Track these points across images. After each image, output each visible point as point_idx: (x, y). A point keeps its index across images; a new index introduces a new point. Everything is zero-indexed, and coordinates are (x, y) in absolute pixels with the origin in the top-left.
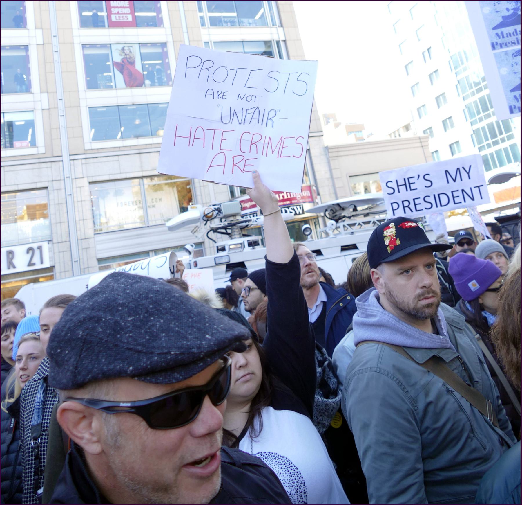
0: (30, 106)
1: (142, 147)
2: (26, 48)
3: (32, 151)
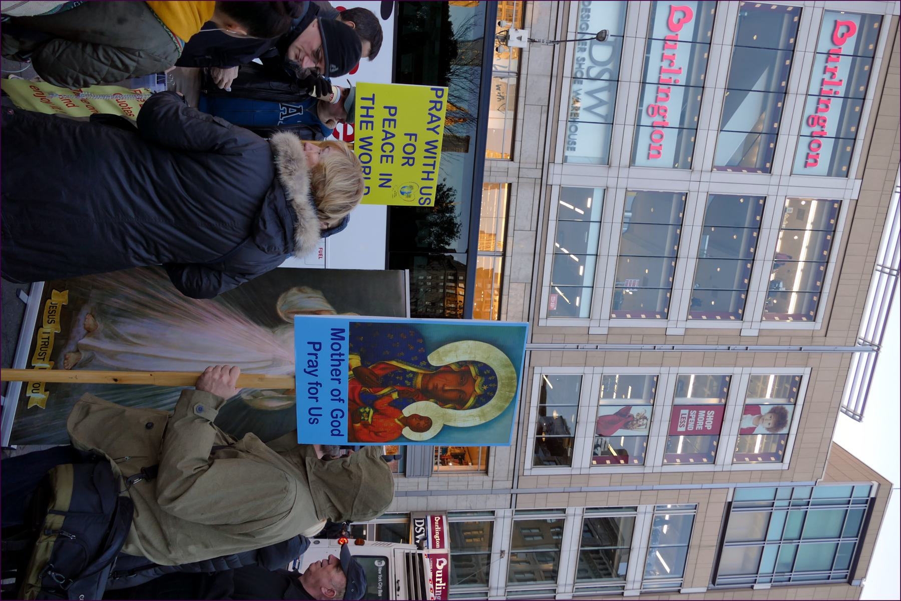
0: (596, 315)
1: (525, 428)
2: (666, 316)
3: (543, 313)
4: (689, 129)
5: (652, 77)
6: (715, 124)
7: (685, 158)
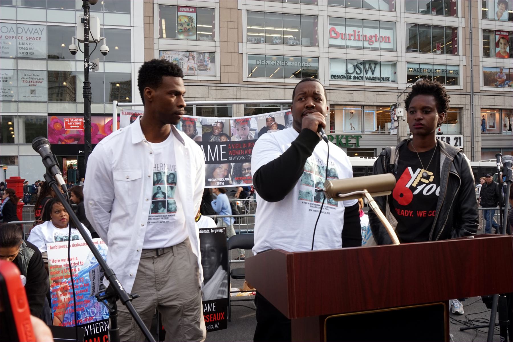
4: (380, 24)
5: (360, 44)
6: (377, 12)
7: (392, 25)
